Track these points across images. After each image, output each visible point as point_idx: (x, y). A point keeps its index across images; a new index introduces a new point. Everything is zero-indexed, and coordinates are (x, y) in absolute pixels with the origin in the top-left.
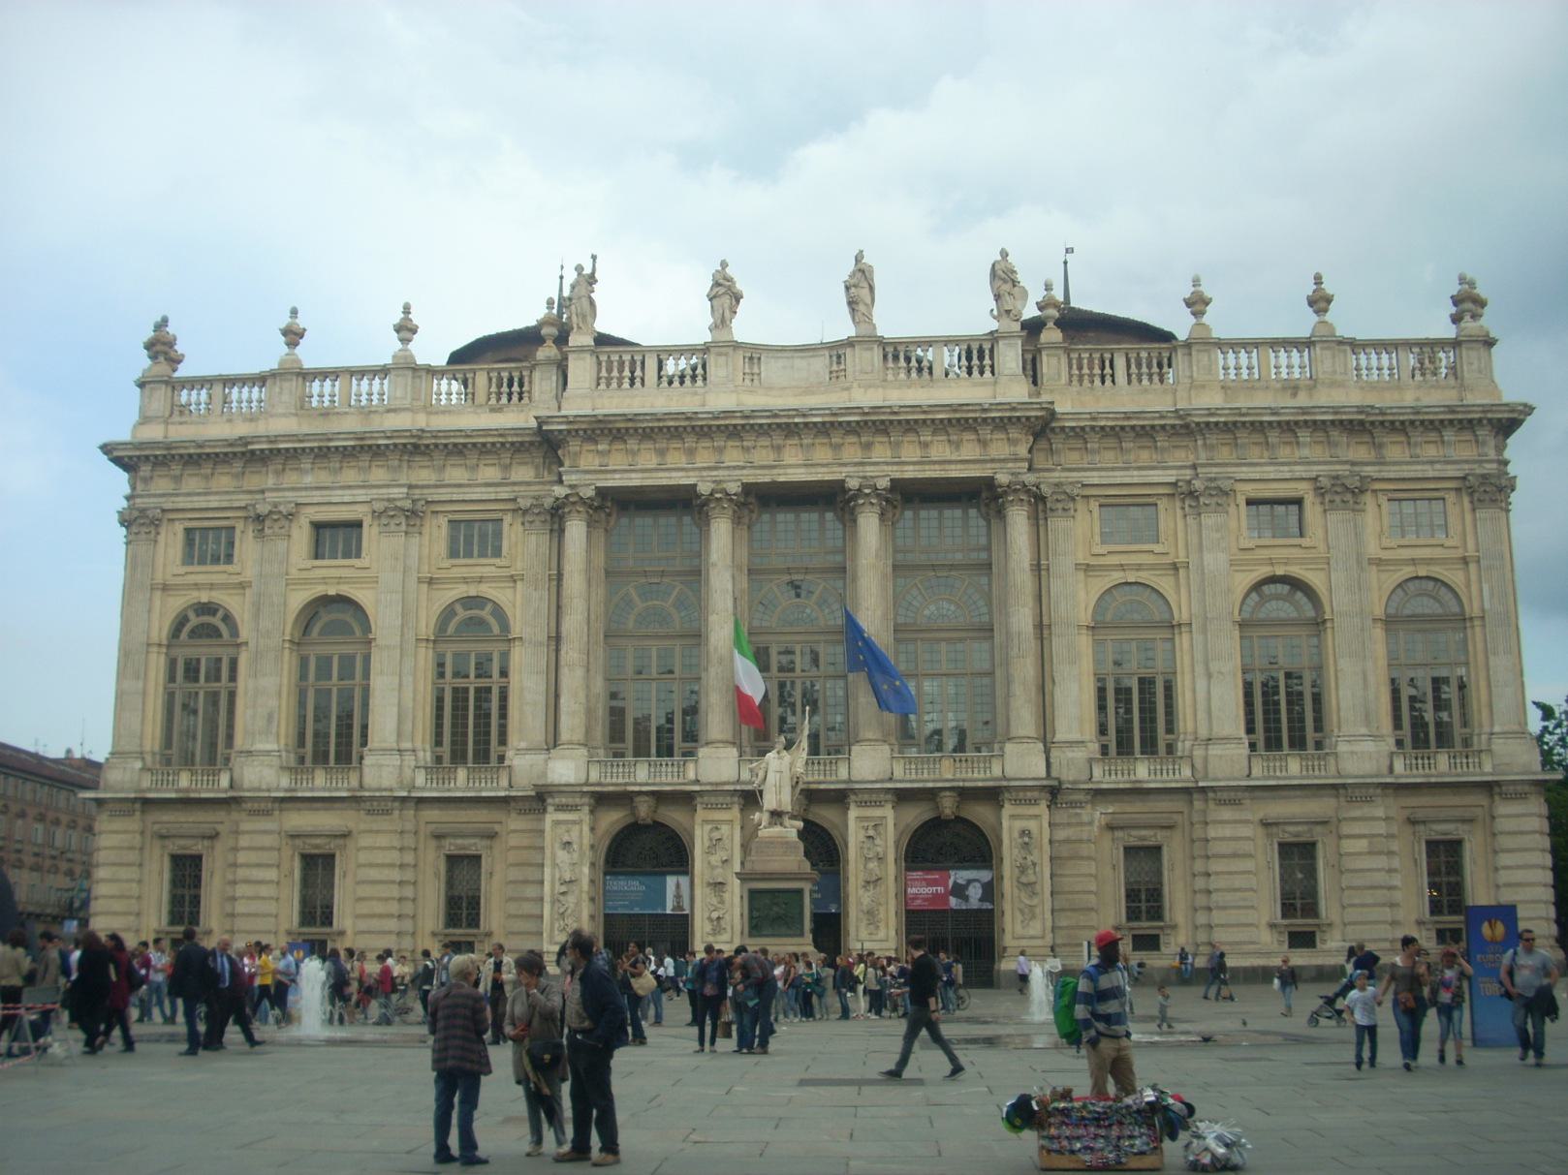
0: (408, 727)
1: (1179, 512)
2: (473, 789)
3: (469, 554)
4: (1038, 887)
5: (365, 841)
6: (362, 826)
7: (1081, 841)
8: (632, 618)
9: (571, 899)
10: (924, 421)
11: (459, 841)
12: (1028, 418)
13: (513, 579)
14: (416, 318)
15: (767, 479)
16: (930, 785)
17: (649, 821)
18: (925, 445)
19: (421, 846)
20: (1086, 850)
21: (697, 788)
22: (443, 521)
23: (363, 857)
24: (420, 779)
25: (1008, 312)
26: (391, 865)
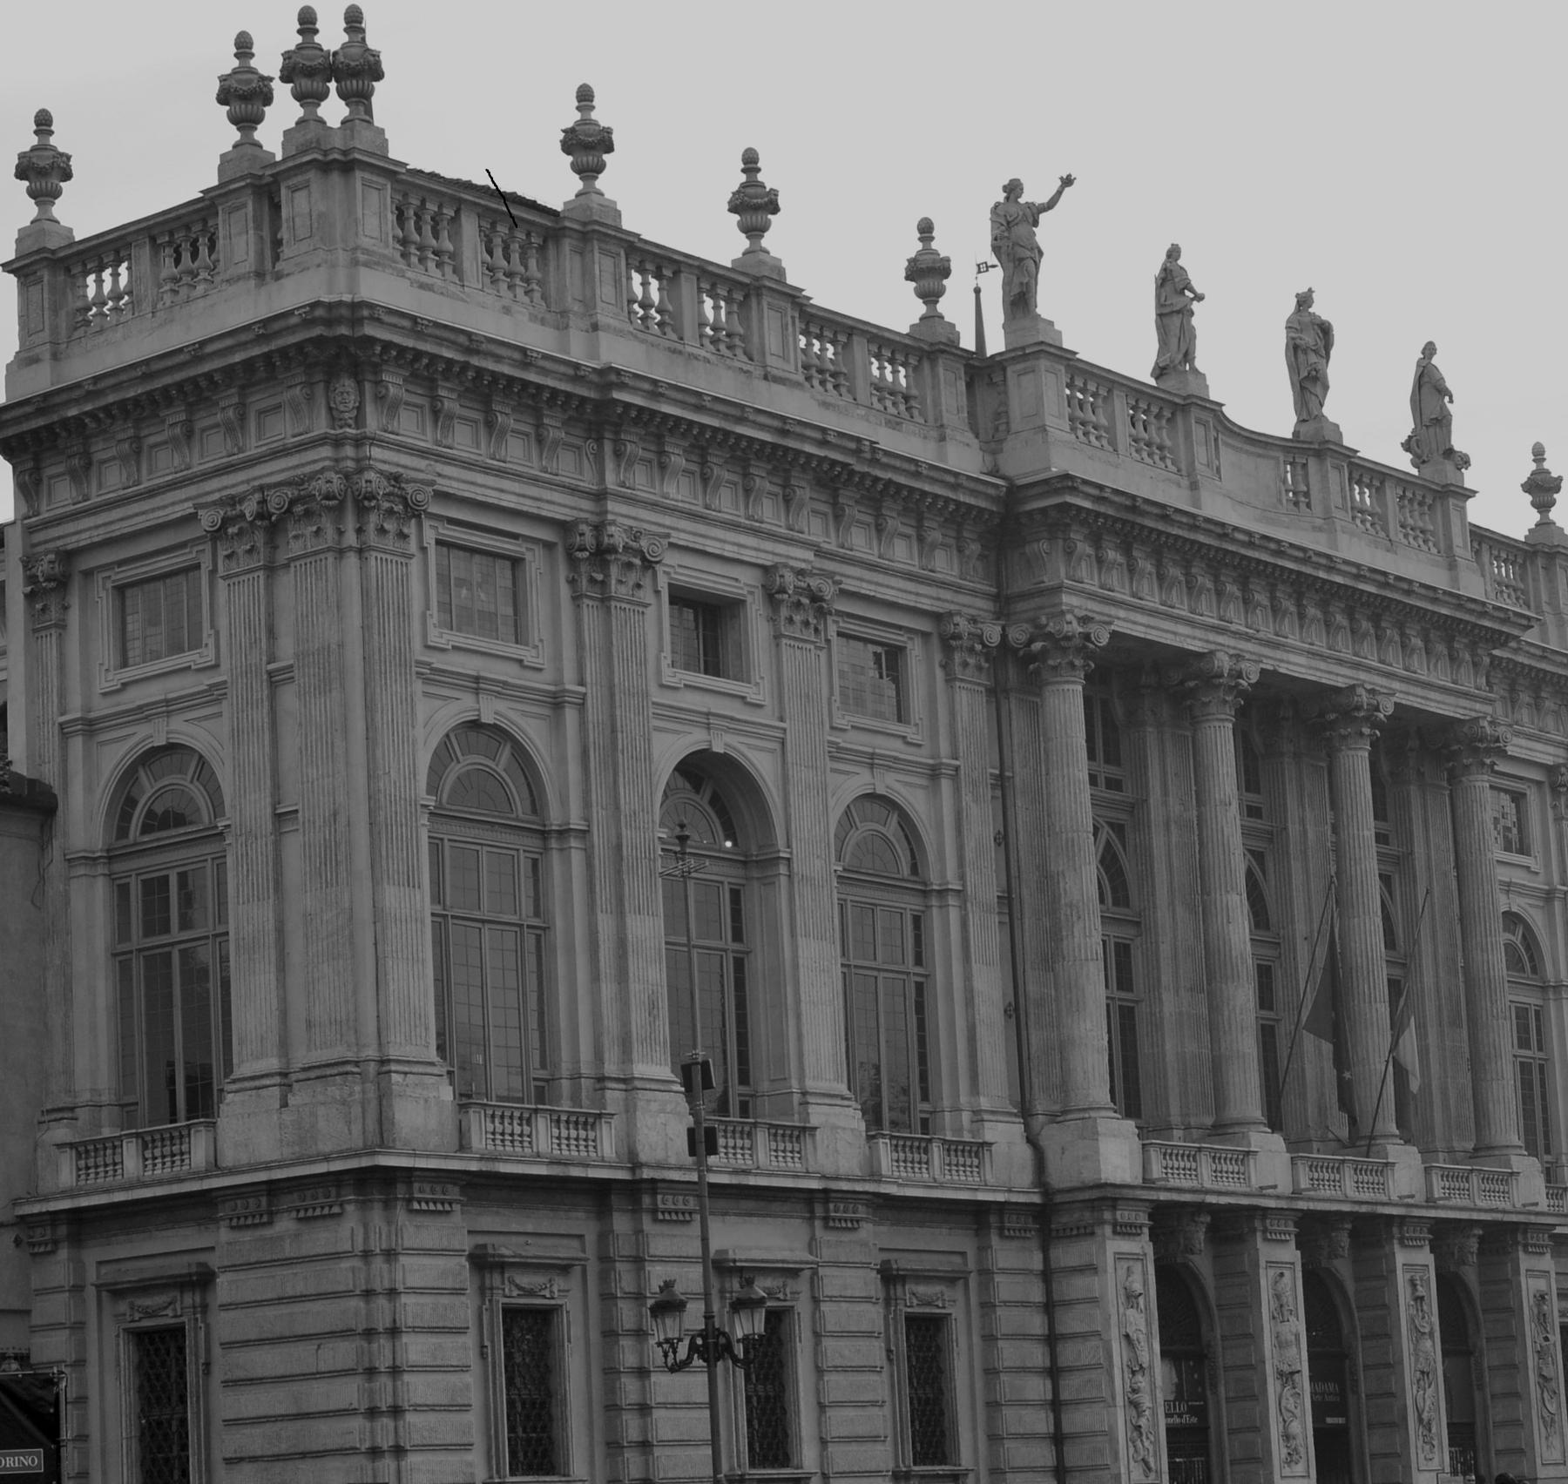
6: (827, 1254)
11: (921, 1289)
13: (934, 773)
21: (1272, 1204)
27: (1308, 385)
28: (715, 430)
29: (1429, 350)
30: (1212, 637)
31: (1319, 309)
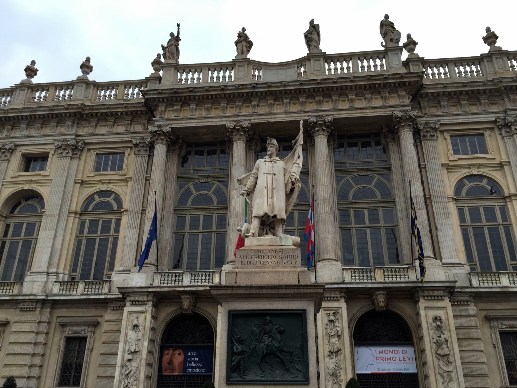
0: (55, 260)
1: (499, 138)
2: (87, 294)
3: (105, 170)
4: (451, 359)
5: (15, 327)
6: (16, 318)
7: (470, 327)
8: (190, 200)
9: (134, 364)
10: (351, 86)
11: (75, 328)
12: (410, 83)
14: (92, 64)
15: (265, 121)
16: (370, 286)
17: (190, 311)
18: (352, 101)
19: (52, 331)
20: (474, 333)
22: (93, 154)
23: (13, 338)
24: (56, 289)
25: (391, 40)
26: (30, 343)
27: (309, 43)
28: (30, 116)
29: (387, 17)
30: (231, 119)
31: (315, 23)
